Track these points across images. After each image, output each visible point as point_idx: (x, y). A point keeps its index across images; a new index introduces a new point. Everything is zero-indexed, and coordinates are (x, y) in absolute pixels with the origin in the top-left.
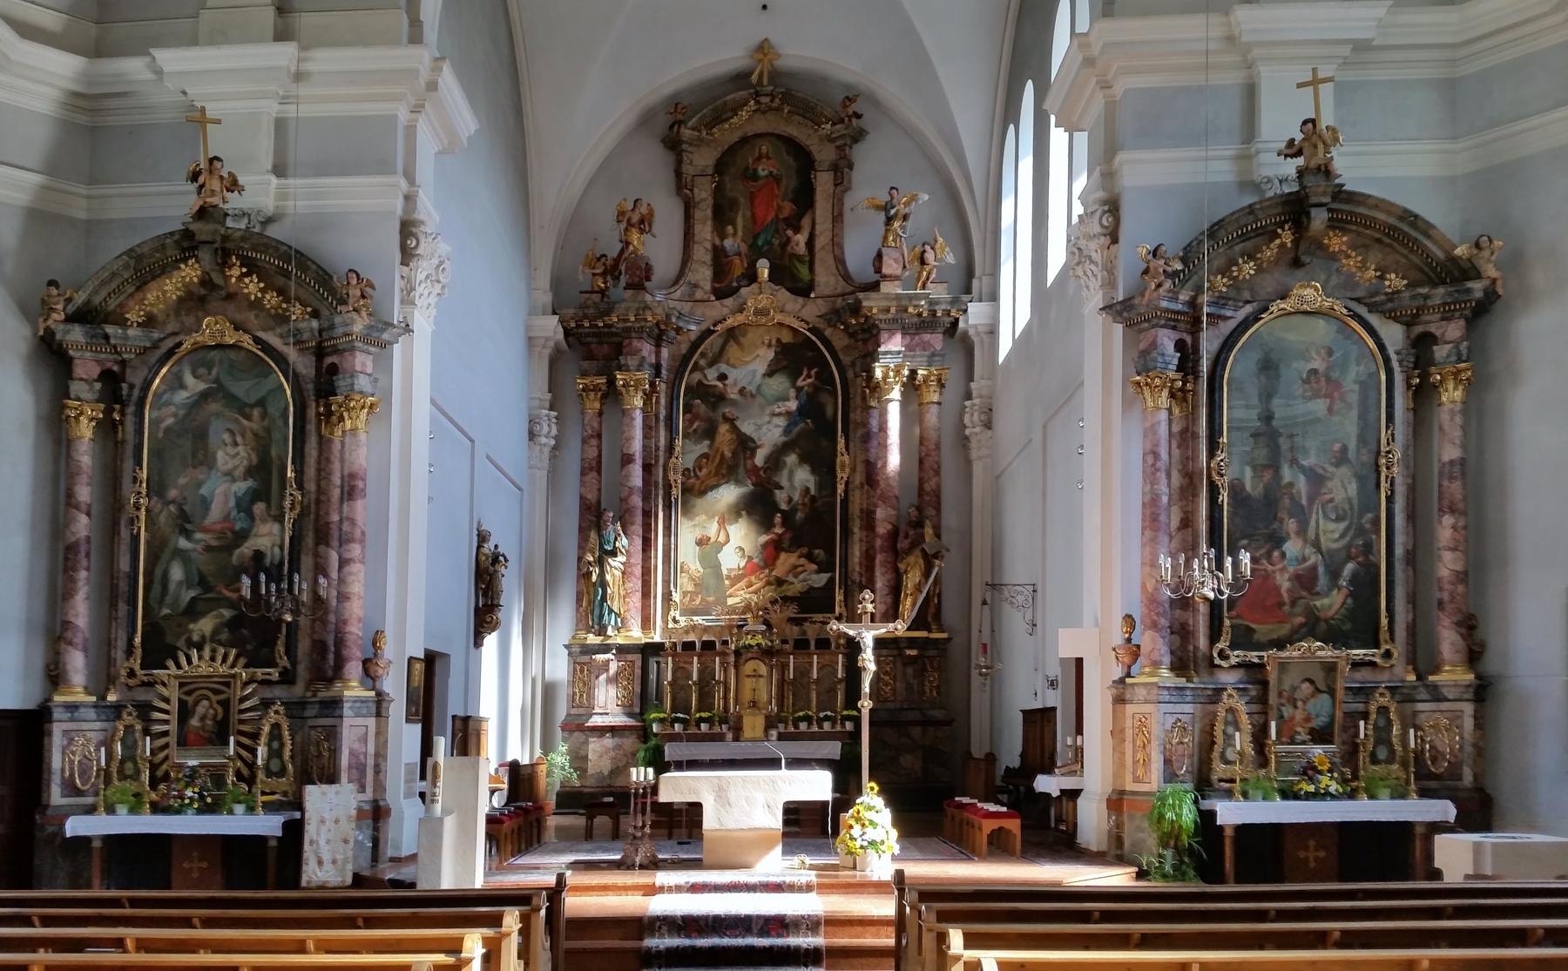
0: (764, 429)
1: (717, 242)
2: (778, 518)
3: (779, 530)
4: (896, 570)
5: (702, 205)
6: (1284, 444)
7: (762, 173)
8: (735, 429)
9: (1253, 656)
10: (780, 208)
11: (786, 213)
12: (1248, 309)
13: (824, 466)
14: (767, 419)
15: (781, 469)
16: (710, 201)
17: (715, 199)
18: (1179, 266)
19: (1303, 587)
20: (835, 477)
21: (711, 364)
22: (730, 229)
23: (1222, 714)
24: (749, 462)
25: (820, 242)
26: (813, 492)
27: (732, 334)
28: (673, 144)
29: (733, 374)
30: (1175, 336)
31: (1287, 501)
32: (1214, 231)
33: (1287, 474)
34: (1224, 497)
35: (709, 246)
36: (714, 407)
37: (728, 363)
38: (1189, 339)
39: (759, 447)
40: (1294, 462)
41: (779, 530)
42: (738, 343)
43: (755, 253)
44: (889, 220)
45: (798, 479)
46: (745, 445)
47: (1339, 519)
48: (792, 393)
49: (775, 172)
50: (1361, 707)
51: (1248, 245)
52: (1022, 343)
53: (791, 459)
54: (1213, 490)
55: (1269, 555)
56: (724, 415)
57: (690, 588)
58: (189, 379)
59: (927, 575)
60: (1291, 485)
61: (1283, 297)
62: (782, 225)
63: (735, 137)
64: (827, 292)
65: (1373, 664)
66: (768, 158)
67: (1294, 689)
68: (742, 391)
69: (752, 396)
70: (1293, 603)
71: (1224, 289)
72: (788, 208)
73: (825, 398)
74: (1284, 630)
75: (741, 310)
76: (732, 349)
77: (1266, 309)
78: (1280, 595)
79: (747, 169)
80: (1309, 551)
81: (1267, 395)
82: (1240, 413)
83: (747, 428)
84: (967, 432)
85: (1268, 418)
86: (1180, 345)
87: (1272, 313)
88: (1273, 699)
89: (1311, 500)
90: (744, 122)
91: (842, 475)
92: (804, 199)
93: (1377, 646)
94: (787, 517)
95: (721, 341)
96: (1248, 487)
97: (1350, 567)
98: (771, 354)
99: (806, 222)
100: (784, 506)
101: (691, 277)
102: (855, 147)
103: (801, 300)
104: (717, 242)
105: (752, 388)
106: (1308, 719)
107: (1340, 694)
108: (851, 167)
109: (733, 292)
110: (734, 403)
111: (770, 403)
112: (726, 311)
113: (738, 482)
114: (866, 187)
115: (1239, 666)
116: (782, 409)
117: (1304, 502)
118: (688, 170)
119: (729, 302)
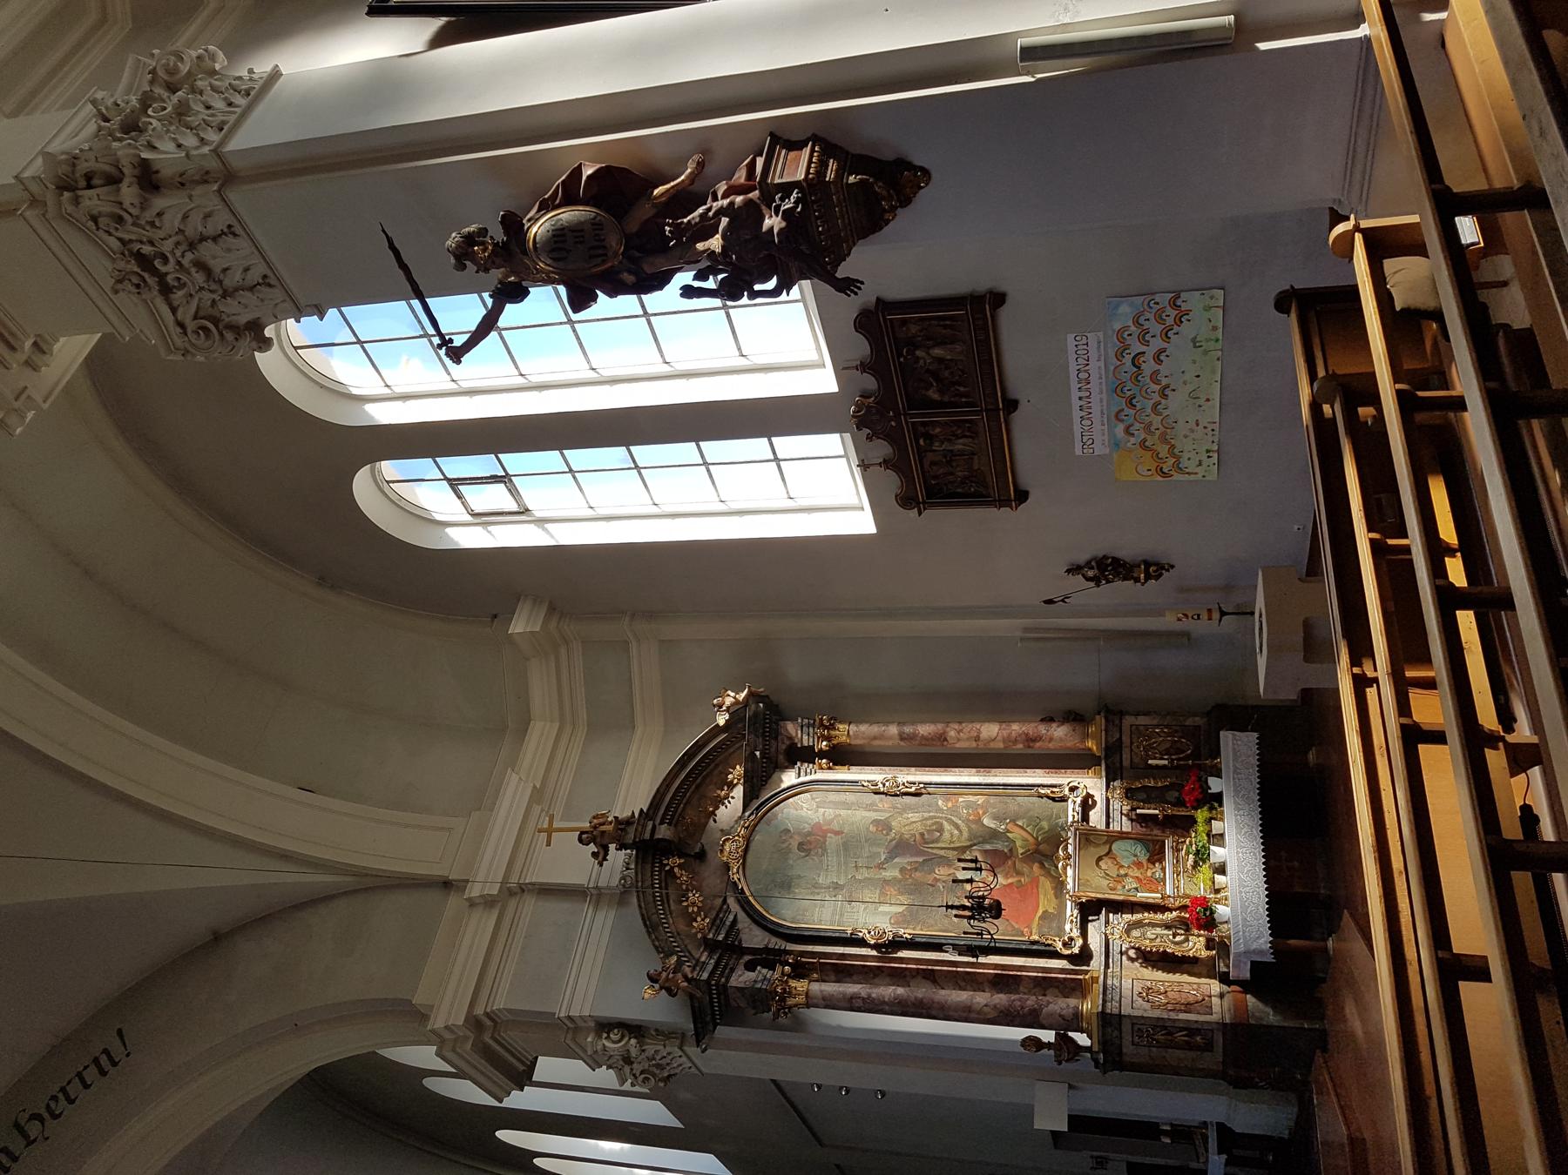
38: (747, 958)
71: (707, 920)
86: (750, 967)
87: (739, 879)
89: (919, 853)
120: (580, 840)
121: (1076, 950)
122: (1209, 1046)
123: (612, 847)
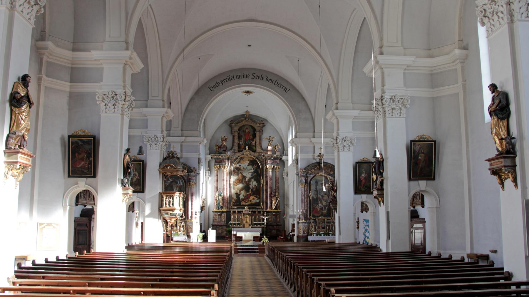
0: (248, 175)
1: (239, 142)
2: (250, 190)
3: (250, 192)
4: (272, 200)
5: (236, 136)
6: (319, 192)
7: (247, 131)
8: (242, 175)
9: (315, 218)
10: (250, 137)
11: (251, 138)
12: (314, 175)
13: (258, 181)
14: (248, 173)
15: (251, 182)
16: (237, 136)
17: (238, 135)
18: (304, 170)
19: (321, 210)
20: (260, 183)
21: (238, 163)
22: (241, 140)
23: (310, 225)
24: (245, 180)
25: (257, 143)
26: (256, 186)
27: (242, 158)
28: (230, 126)
29: (242, 165)
30: (305, 178)
31: (319, 199)
32: (308, 166)
33: (319, 196)
34: (311, 198)
35: (237, 143)
36: (238, 171)
37: (241, 163)
38: (306, 178)
39: (246, 178)
40: (320, 194)
41: (250, 192)
42: (243, 160)
43: (246, 145)
44: (269, 142)
45: (254, 183)
46: (244, 177)
47: (325, 201)
48: (253, 169)
49: (249, 131)
50: (329, 225)
51: (313, 167)
52: (291, 165)
53: (253, 180)
54: (310, 198)
55: (317, 206)
56: (240, 172)
57: (234, 201)
58: (170, 179)
59: (276, 201)
60: (319, 197)
61: (318, 174)
62: (250, 140)
63: (242, 125)
64: (258, 152)
65: (330, 219)
66: (248, 129)
67: (320, 222)
68: (243, 168)
69: (245, 169)
70: (320, 212)
72: (251, 137)
73: (258, 170)
74: (319, 215)
75: (243, 155)
76: (242, 161)
77: (316, 175)
78: (318, 211)
79: (244, 130)
80: (322, 205)
81: (316, 186)
82: (313, 188)
83: (244, 174)
84: (284, 177)
85: (316, 188)
86: (305, 179)
88: (317, 224)
89: (322, 199)
90: (244, 123)
91: (261, 183)
92: (254, 136)
93: (330, 217)
94: (252, 190)
95: (239, 159)
96: (314, 197)
97: (327, 207)
98: (249, 162)
99: (255, 140)
100: (251, 188)
101: (234, 148)
102: (263, 128)
103: (254, 153)
104: (239, 142)
105: (245, 168)
106: (322, 226)
107: (326, 223)
108: (262, 131)
109: (241, 151)
110: (242, 170)
111: (249, 170)
112: (240, 154)
113: (243, 184)
114: (265, 135)
115: (313, 219)
116: (251, 171)
117: (321, 199)
118: (233, 130)
119: (241, 153)
120: (320, 153)
121: (310, 219)
122: (300, 234)
123: (319, 158)
